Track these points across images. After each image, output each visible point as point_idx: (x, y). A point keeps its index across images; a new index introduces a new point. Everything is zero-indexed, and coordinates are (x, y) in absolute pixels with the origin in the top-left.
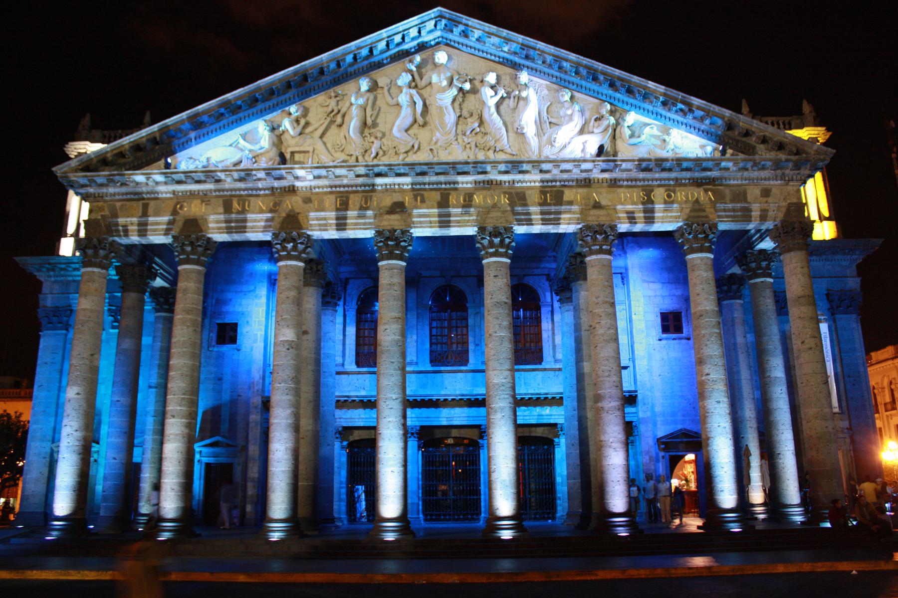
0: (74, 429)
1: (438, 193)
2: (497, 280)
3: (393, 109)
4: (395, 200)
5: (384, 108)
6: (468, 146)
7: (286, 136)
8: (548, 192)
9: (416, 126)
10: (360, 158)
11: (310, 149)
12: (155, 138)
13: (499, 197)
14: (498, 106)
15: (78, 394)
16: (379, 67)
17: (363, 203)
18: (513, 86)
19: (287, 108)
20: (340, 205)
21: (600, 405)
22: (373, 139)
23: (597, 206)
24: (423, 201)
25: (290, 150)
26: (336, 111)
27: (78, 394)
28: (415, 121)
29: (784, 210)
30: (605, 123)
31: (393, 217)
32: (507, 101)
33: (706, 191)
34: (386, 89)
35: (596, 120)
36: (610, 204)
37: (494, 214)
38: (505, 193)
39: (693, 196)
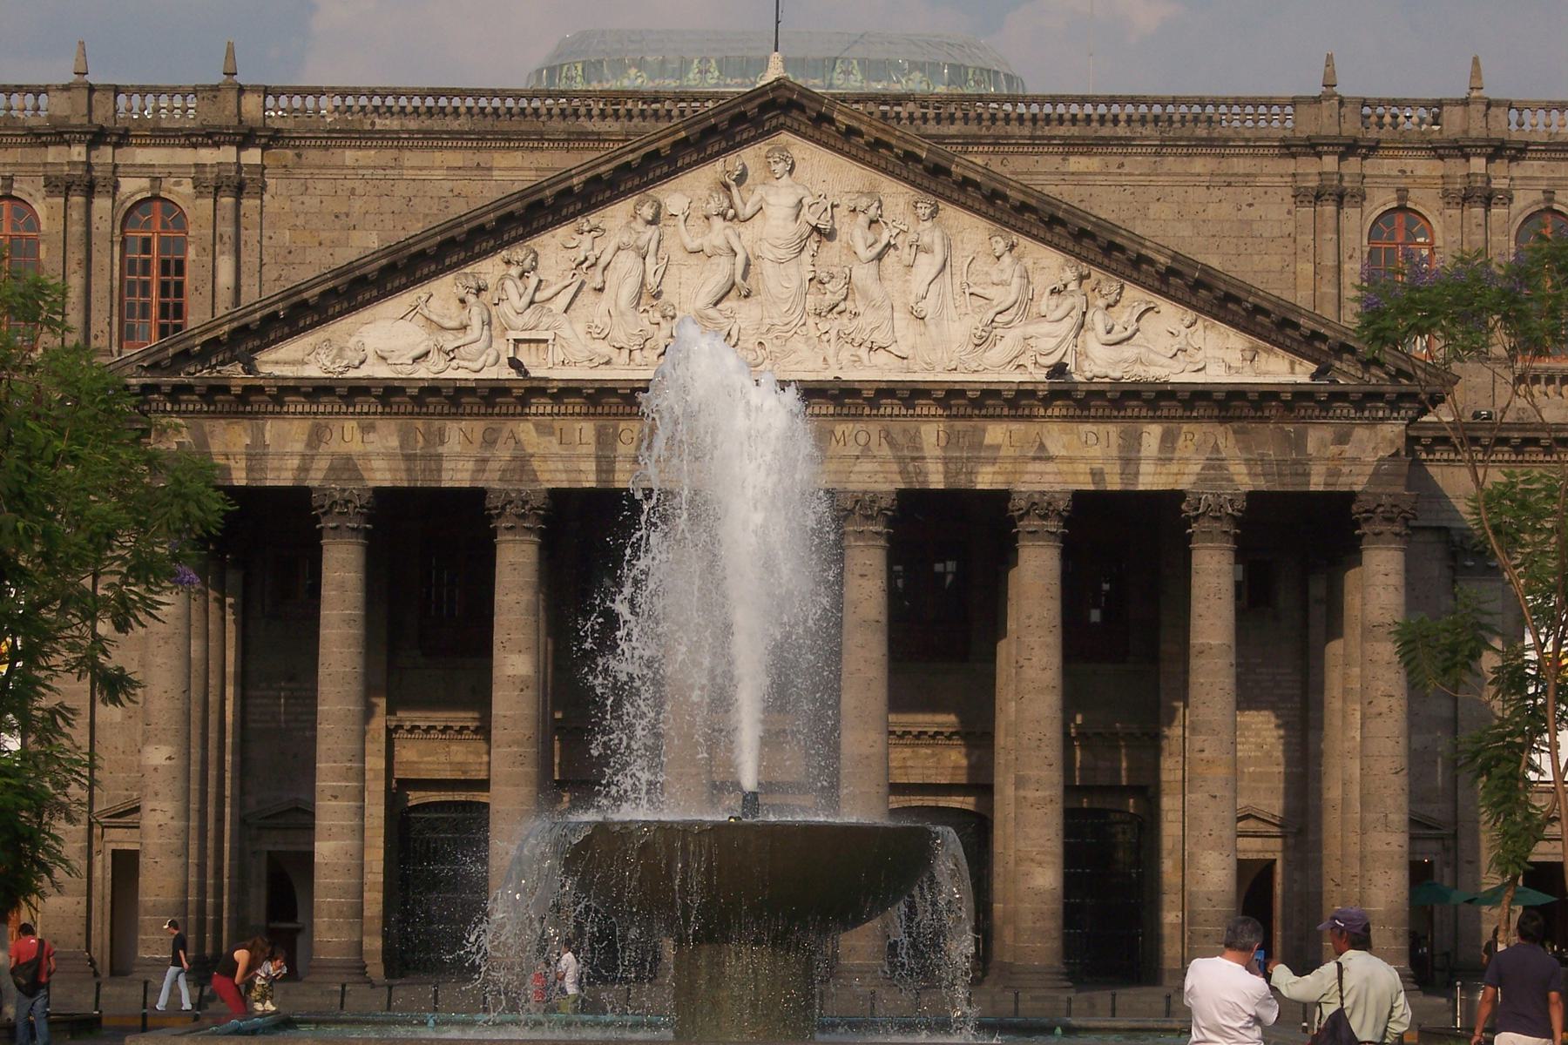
0: (169, 814)
2: (860, 581)
3: (693, 259)
5: (678, 256)
6: (825, 338)
7: (504, 307)
10: (637, 354)
11: (548, 335)
14: (879, 257)
15: (170, 758)
18: (910, 219)
21: (1022, 793)
22: (657, 317)
23: (1043, 456)
25: (512, 335)
26: (592, 260)
27: (170, 758)
28: (734, 284)
29: (1370, 470)
30: (1067, 304)
34: (682, 218)
36: (1063, 453)
37: (867, 466)
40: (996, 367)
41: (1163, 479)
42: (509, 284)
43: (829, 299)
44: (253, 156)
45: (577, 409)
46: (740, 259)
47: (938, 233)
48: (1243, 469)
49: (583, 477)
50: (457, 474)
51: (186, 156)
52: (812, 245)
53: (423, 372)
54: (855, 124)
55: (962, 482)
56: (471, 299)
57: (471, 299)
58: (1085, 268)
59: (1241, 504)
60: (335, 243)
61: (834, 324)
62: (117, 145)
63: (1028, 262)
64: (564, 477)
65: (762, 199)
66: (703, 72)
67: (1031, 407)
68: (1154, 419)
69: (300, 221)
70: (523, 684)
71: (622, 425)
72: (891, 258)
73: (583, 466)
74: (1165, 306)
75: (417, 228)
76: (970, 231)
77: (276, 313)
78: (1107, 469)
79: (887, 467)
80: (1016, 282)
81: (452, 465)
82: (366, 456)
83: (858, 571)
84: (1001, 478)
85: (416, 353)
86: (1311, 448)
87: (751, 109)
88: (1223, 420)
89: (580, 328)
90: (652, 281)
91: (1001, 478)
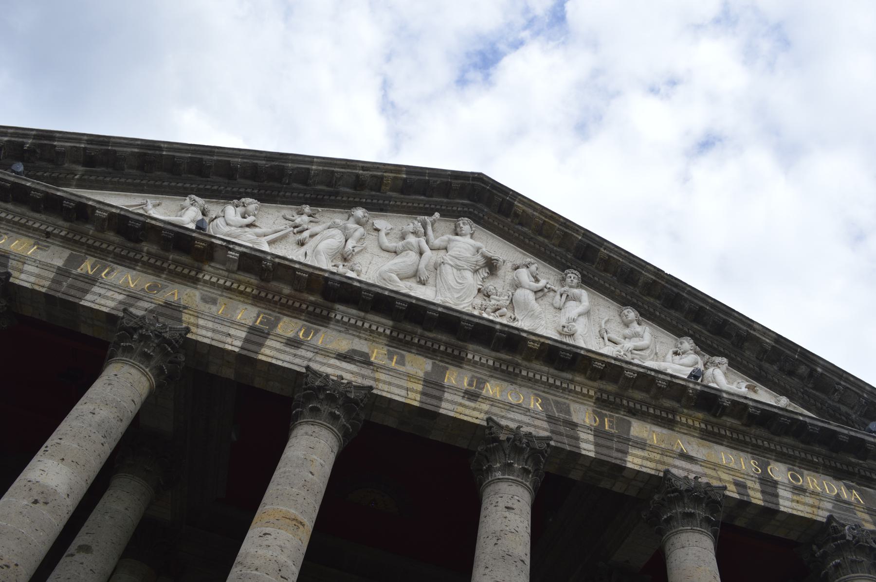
1: (430, 362)
2: (507, 514)
4: (356, 348)
8: (606, 415)
9: (413, 280)
12: (22, 144)
16: (381, 210)
17: (301, 334)
20: (261, 323)
24: (401, 362)
31: (344, 365)
33: (849, 488)
35: (676, 353)
41: (801, 507)
45: (249, 290)
48: (867, 517)
49: (229, 340)
50: (103, 299)
52: (484, 273)
55: (613, 457)
64: (209, 334)
65: (449, 241)
67: (674, 412)
68: (782, 458)
70: (42, 498)
71: (286, 319)
73: (232, 332)
77: (22, 144)
78: (749, 484)
79: (538, 423)
81: (102, 291)
82: (23, 260)
83: (502, 505)
84: (652, 465)
87: (456, 183)
88: (839, 474)
91: (652, 465)
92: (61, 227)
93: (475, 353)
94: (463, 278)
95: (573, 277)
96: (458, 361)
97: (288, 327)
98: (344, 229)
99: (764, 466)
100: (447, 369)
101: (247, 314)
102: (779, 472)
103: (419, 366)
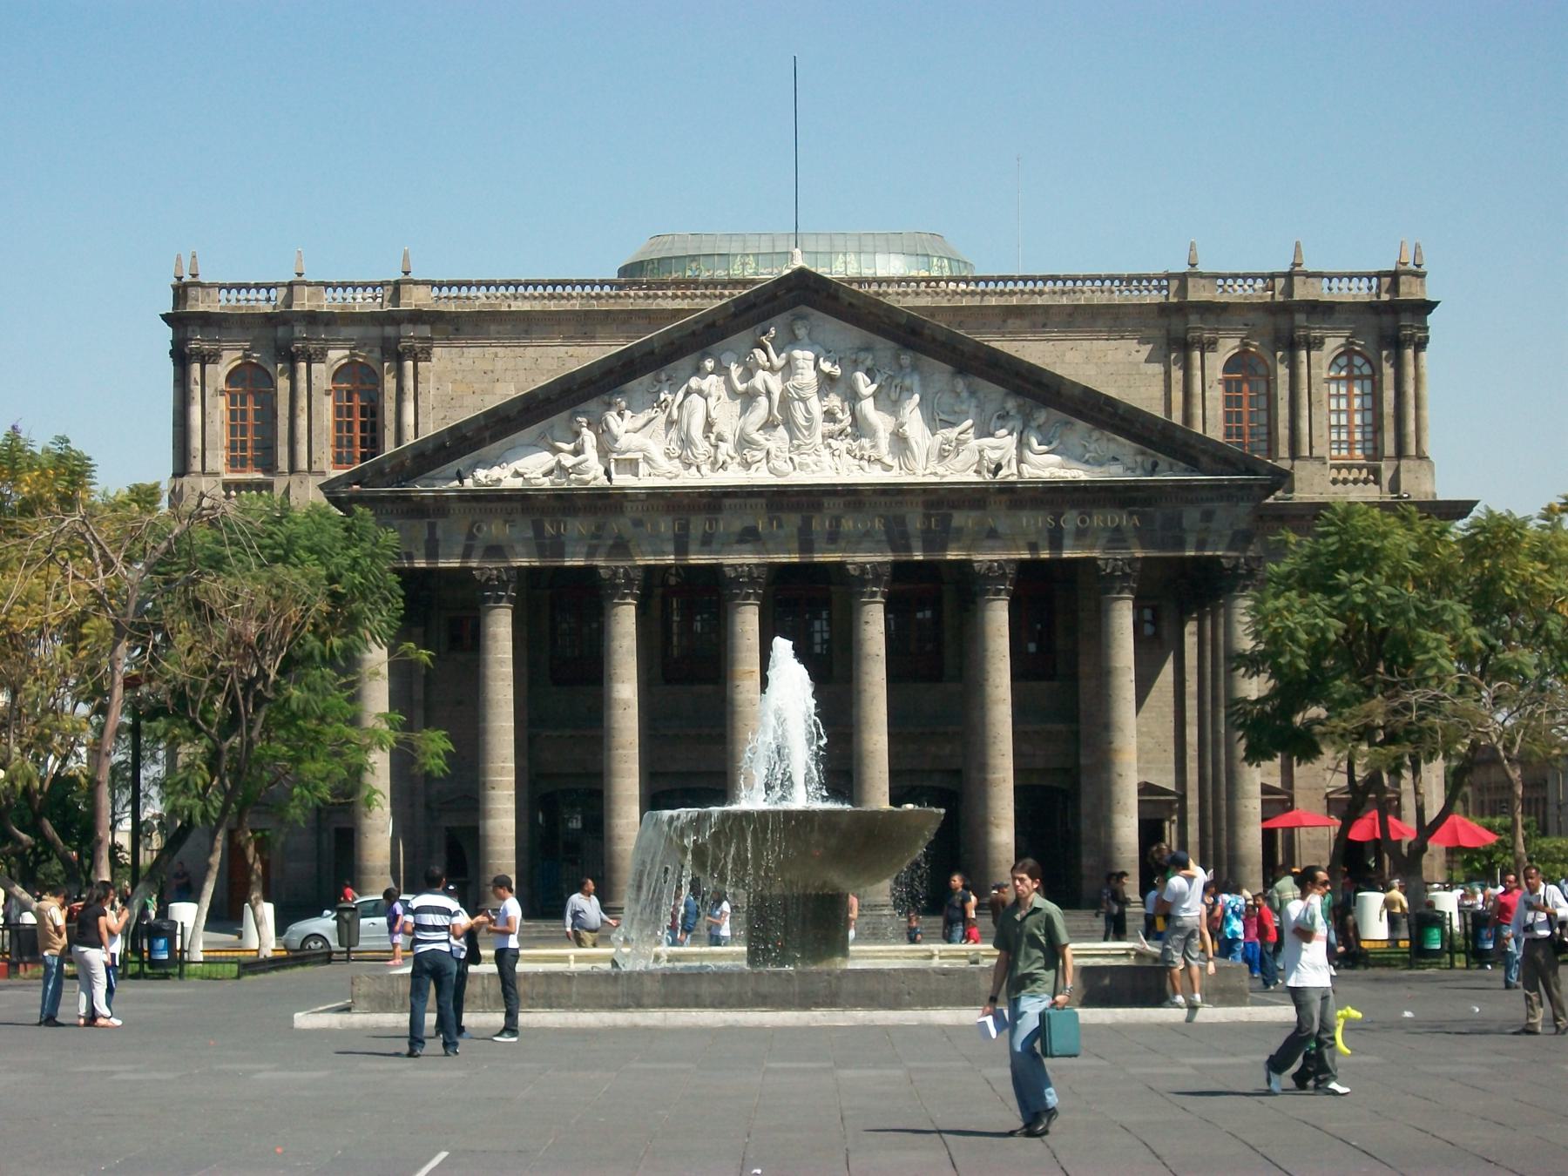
7: (606, 436)
11: (639, 455)
13: (872, 521)
19: (606, 398)
24: (780, 526)
25: (615, 456)
32: (884, 391)
33: (1131, 514)
35: (999, 417)
38: (881, 516)
39: (1113, 521)
40: (960, 471)
42: (610, 419)
43: (837, 427)
44: (426, 331)
46: (776, 397)
47: (916, 378)
51: (374, 331)
53: (546, 483)
54: (854, 301)
56: (585, 430)
57: (585, 430)
58: (1021, 401)
59: (1138, 565)
60: (484, 392)
61: (841, 445)
62: (327, 324)
63: (981, 395)
66: (744, 265)
69: (459, 377)
72: (883, 396)
74: (1081, 425)
75: (543, 381)
76: (940, 372)
80: (973, 411)
85: (545, 468)
86: (1186, 523)
89: (663, 447)
90: (713, 415)
92: (518, 505)
93: (826, 501)
94: (808, 411)
95: (906, 359)
96: (818, 507)
97: (698, 525)
98: (700, 392)
99: (1057, 517)
100: (811, 518)
101: (665, 526)
102: (1071, 520)
103: (793, 521)
